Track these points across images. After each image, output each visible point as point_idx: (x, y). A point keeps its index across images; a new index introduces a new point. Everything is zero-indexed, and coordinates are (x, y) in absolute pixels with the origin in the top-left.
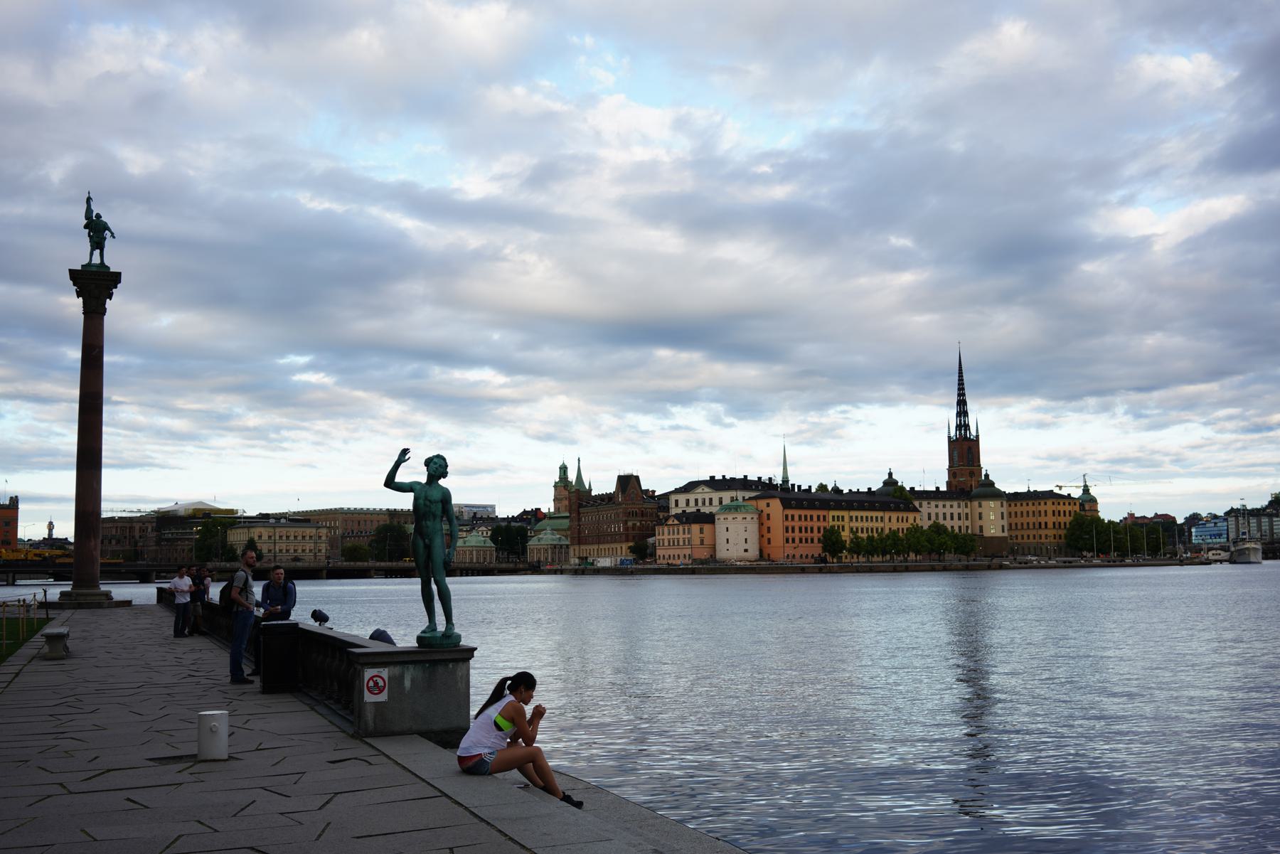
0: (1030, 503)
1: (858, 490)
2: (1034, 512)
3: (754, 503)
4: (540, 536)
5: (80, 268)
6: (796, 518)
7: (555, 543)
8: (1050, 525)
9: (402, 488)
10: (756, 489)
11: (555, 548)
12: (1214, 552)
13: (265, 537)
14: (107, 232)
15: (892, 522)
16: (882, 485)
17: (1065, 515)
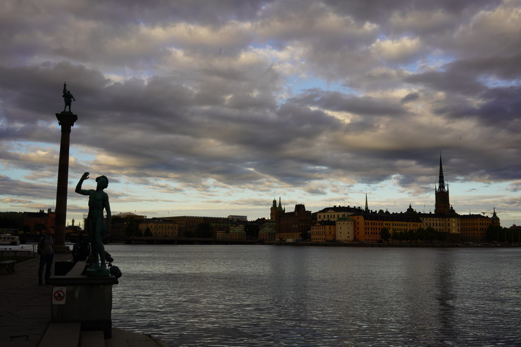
1: (397, 213)
2: (472, 223)
3: (352, 217)
4: (264, 229)
5: (60, 113)
6: (370, 224)
7: (270, 232)
8: (479, 229)
9: (85, 193)
10: (353, 212)
11: (270, 234)
13: (153, 227)
14: (72, 98)
15: (411, 226)
16: (407, 211)
17: (485, 225)
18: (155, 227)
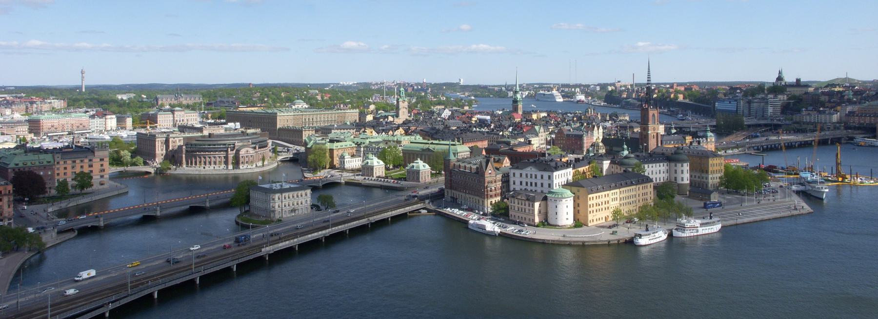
6: (595, 198)
12: (795, 185)
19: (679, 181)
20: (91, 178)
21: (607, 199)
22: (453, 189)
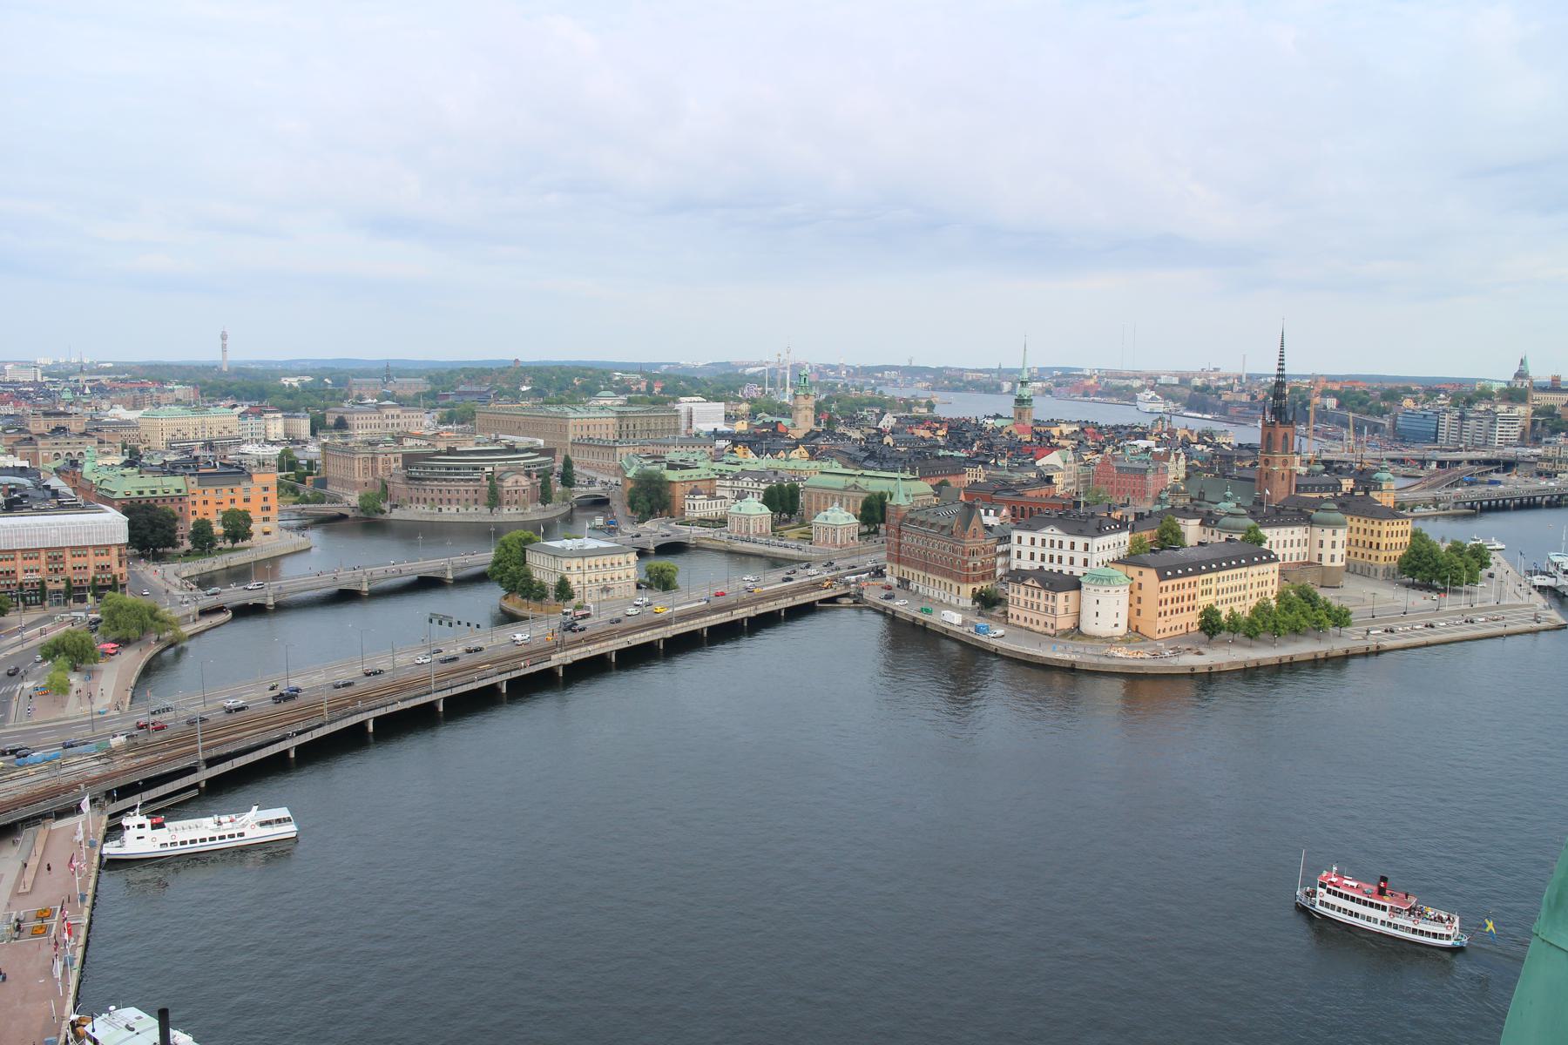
0: (1362, 520)
6: (1170, 589)
8: (1382, 547)
13: (574, 568)
18: (579, 567)
19: (1326, 562)
20: (250, 521)
21: (1192, 591)
22: (903, 564)
